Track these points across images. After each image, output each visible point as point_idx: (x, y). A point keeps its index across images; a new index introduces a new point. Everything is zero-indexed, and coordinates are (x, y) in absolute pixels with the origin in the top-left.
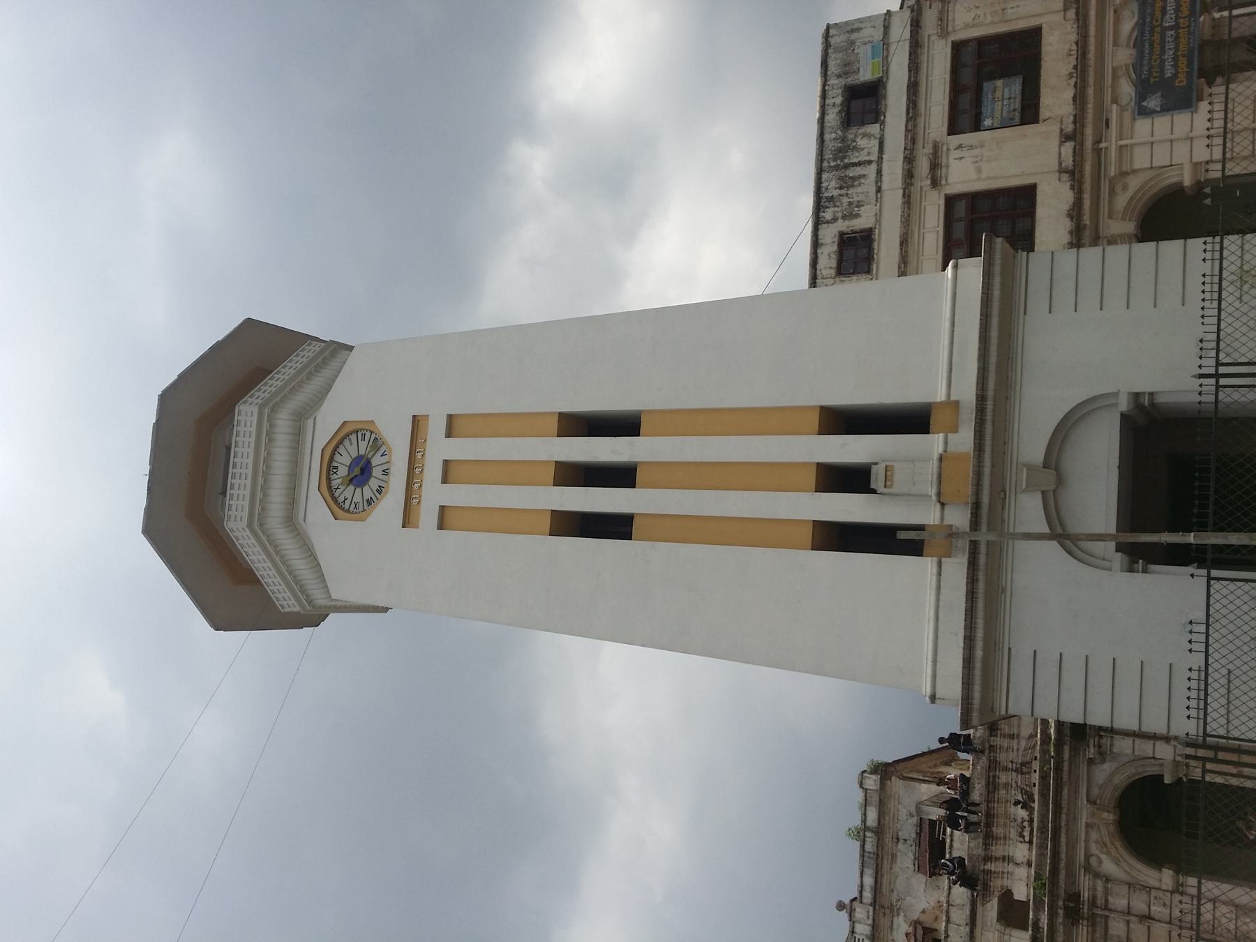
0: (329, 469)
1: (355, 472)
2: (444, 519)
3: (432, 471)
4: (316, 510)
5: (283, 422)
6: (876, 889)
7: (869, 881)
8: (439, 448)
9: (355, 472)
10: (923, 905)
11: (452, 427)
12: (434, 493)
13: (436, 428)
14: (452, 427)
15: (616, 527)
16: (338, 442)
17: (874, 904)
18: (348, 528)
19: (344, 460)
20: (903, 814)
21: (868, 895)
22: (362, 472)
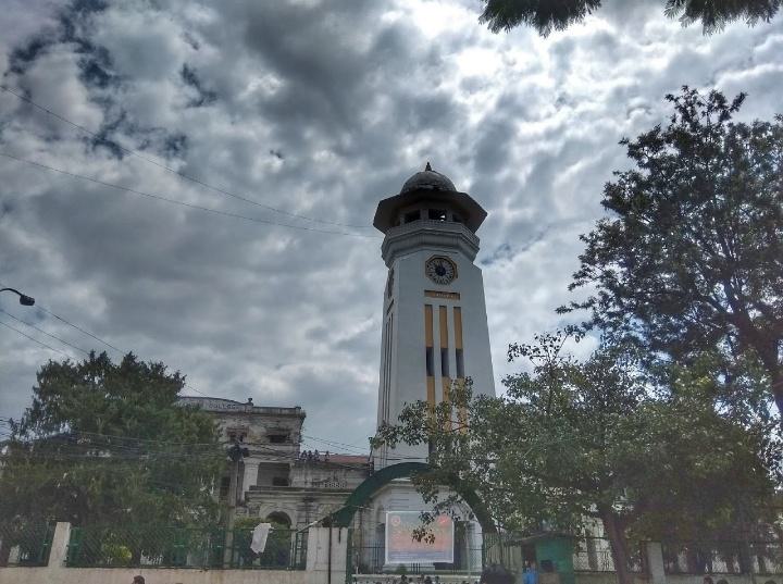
0: (440, 258)
1: (441, 270)
2: (429, 307)
3: (443, 301)
4: (428, 254)
5: (454, 241)
6: (258, 413)
7: (261, 410)
8: (450, 304)
9: (441, 270)
10: (255, 431)
11: (457, 309)
12: (436, 302)
13: (457, 303)
14: (457, 309)
15: (430, 372)
16: (450, 262)
17: (253, 413)
18: (422, 269)
19: (445, 264)
20: (288, 423)
21: (256, 410)
22: (440, 271)
